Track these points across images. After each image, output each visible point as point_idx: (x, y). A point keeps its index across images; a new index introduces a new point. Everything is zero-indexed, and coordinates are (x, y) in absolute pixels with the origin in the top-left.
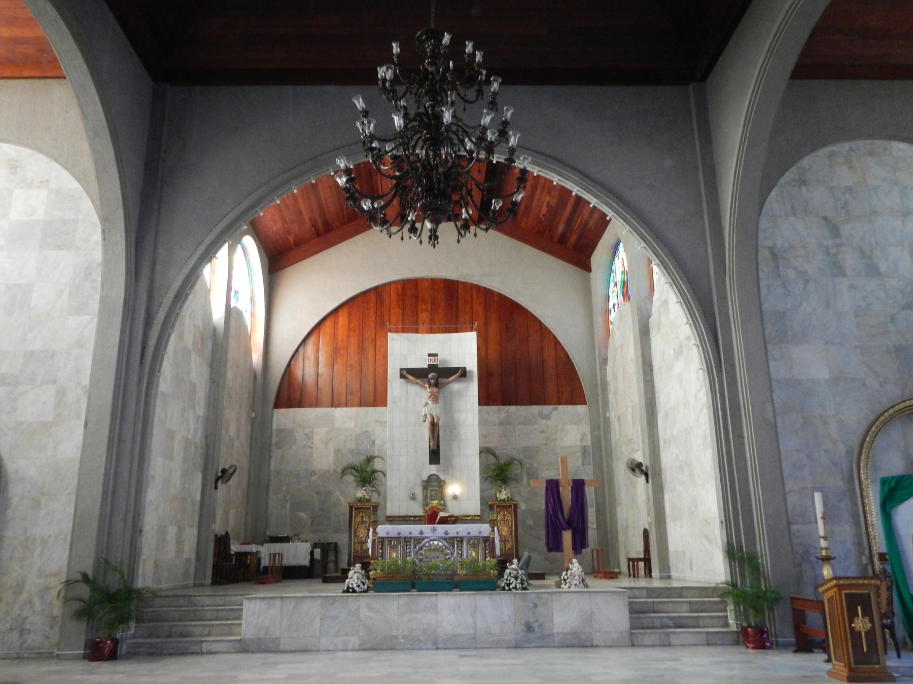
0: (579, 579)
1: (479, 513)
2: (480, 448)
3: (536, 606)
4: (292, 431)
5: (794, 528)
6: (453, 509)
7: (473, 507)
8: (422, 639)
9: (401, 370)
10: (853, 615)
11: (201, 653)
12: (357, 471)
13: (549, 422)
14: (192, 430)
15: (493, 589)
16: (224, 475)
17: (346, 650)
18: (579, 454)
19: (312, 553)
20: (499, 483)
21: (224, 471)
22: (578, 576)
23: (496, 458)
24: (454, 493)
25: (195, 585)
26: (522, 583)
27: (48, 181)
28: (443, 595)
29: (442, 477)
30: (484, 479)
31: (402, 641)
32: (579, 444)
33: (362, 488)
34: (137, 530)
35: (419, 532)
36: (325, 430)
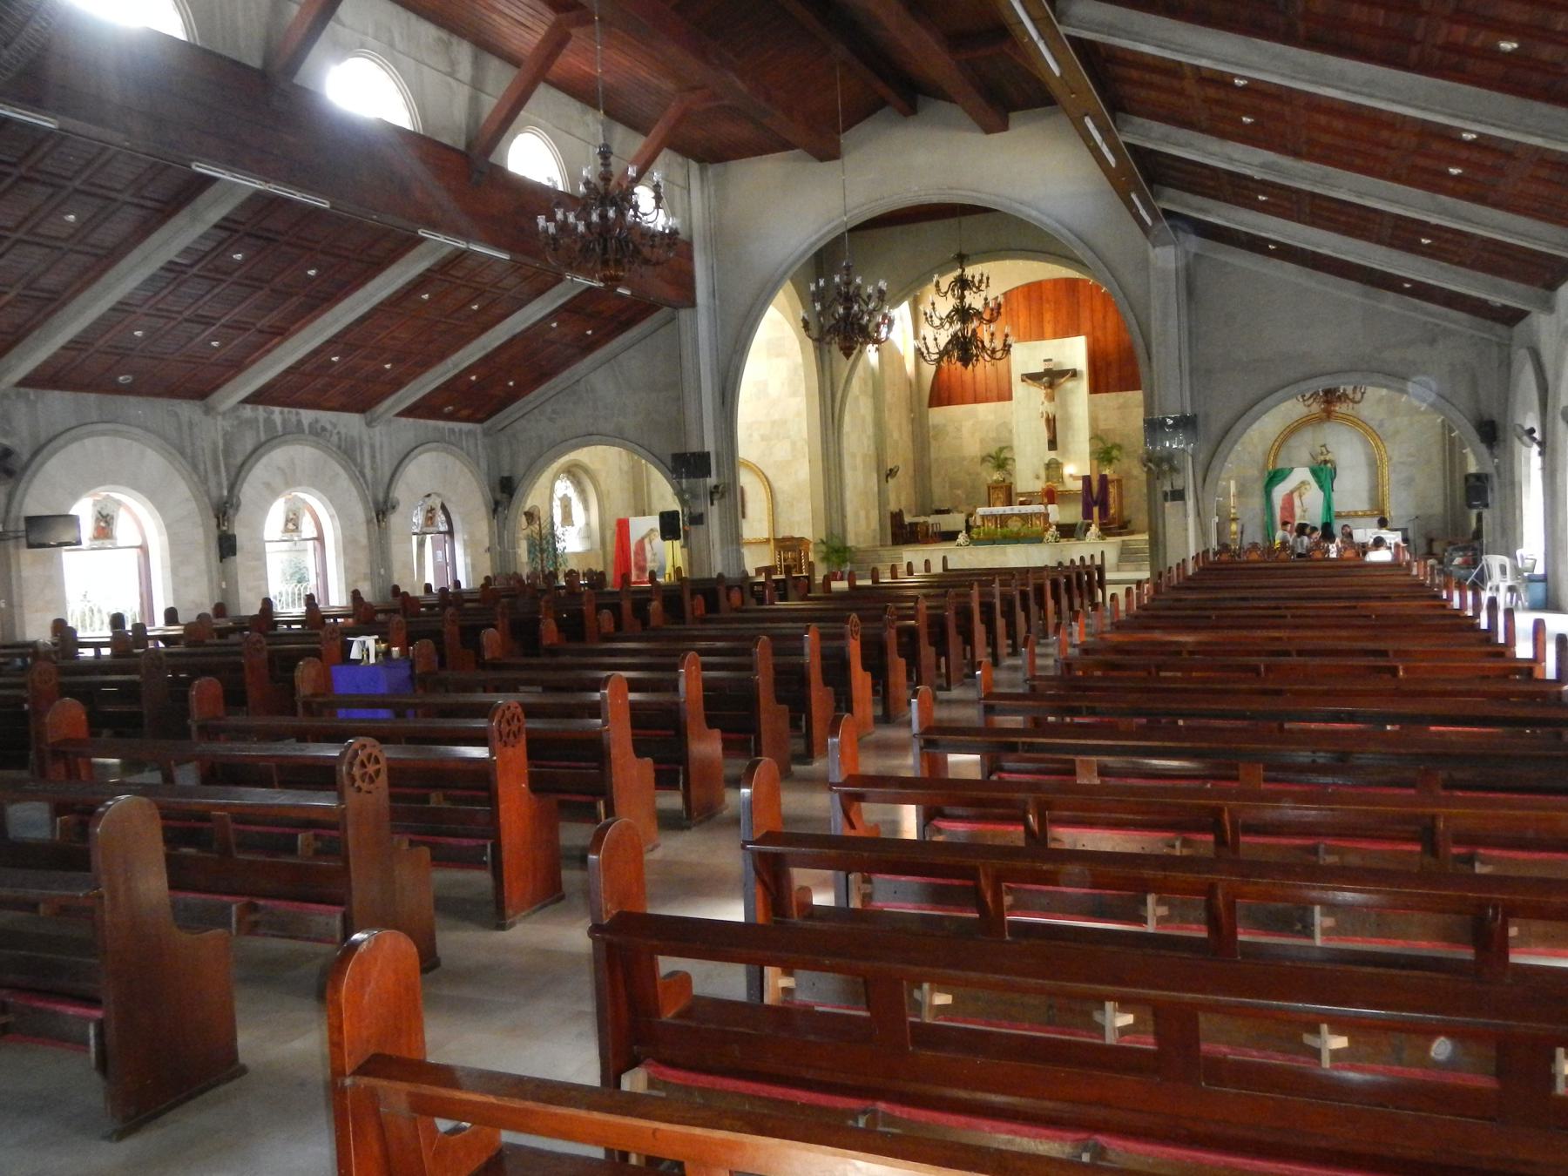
4: (945, 426)
9: (1023, 375)
12: (992, 457)
16: (892, 473)
21: (891, 470)
25: (881, 546)
29: (1060, 460)
34: (844, 516)
36: (971, 422)
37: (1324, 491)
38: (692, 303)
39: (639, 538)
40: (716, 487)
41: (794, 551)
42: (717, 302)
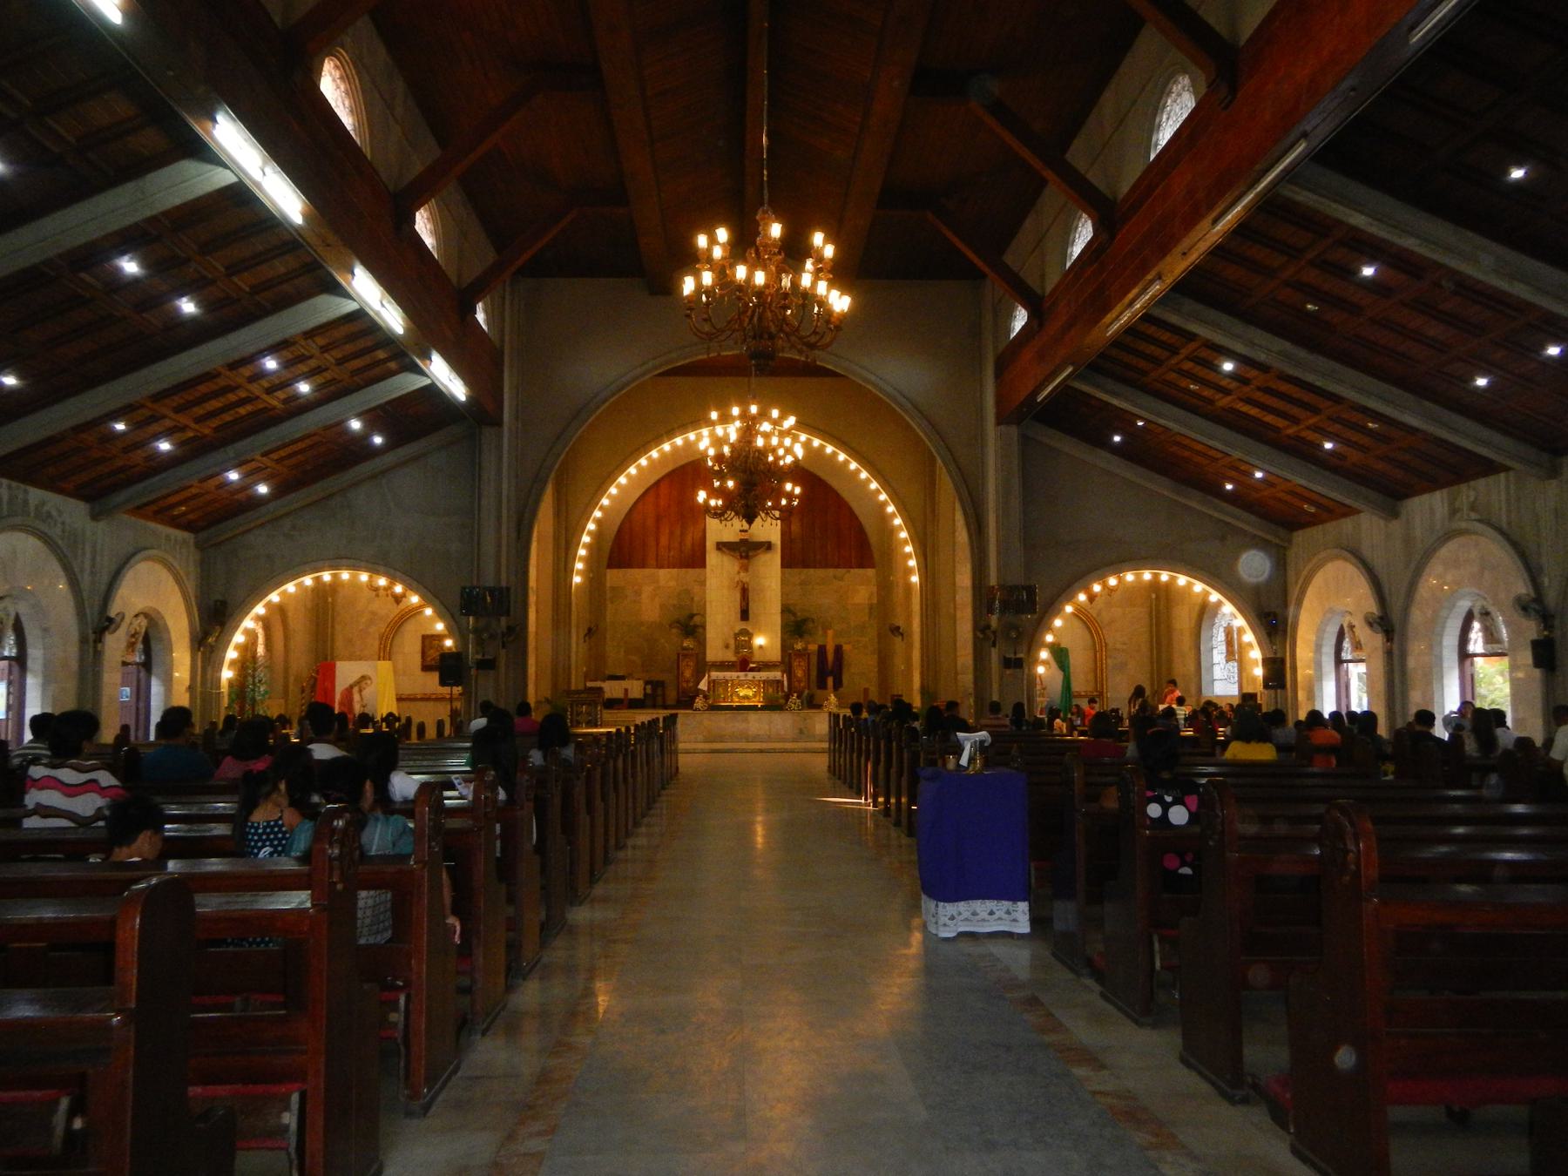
1: (779, 659)
2: (782, 605)
3: (805, 719)
5: (959, 677)
6: (758, 657)
7: (775, 655)
12: (680, 624)
13: (842, 583)
18: (867, 611)
19: (645, 689)
20: (797, 636)
21: (590, 630)
23: (794, 614)
29: (751, 631)
30: (783, 633)
32: (867, 602)
37: (1063, 671)
38: (498, 423)
39: (347, 686)
40: (509, 628)
41: (589, 704)
42: (520, 425)
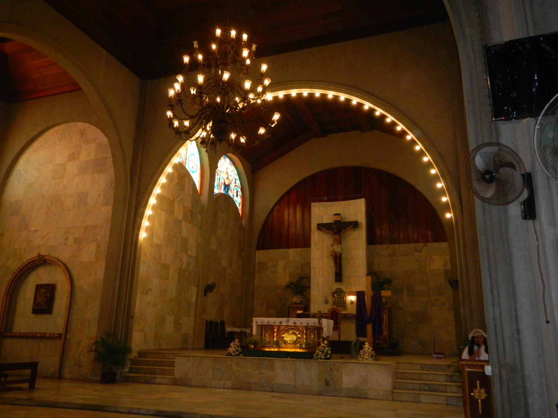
0: (368, 355)
3: (332, 370)
8: (265, 385)
9: (318, 225)
10: (472, 387)
11: (155, 383)
14: (185, 264)
15: (311, 359)
17: (224, 388)
22: (368, 353)
24: (351, 300)
26: (325, 356)
27: (96, 139)
28: (277, 360)
29: (344, 289)
31: (254, 385)
32: (442, 268)
33: (296, 296)
35: (279, 322)
36: (284, 262)
